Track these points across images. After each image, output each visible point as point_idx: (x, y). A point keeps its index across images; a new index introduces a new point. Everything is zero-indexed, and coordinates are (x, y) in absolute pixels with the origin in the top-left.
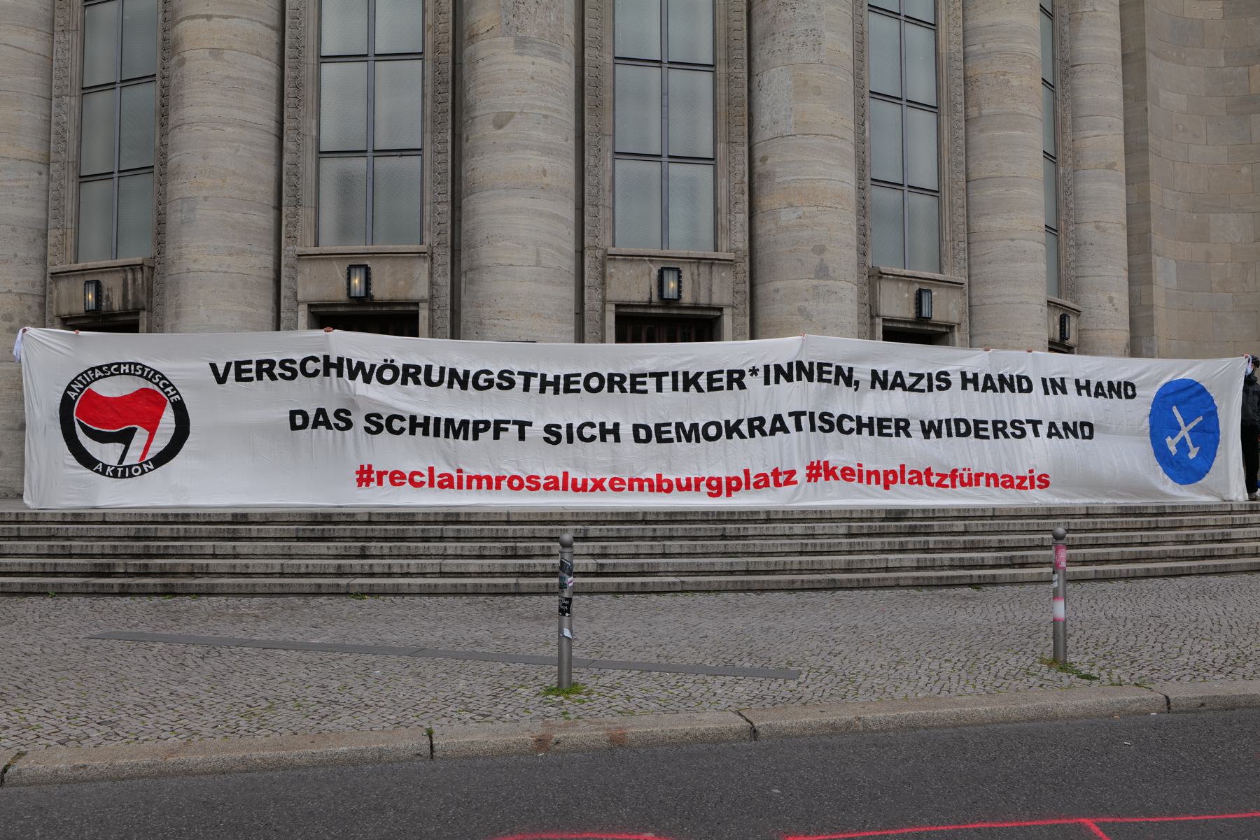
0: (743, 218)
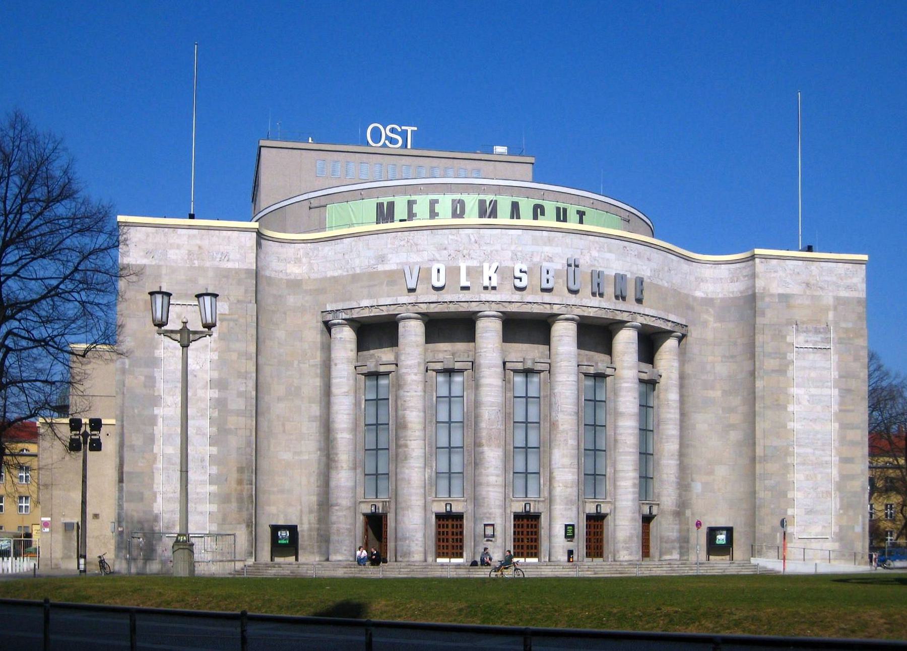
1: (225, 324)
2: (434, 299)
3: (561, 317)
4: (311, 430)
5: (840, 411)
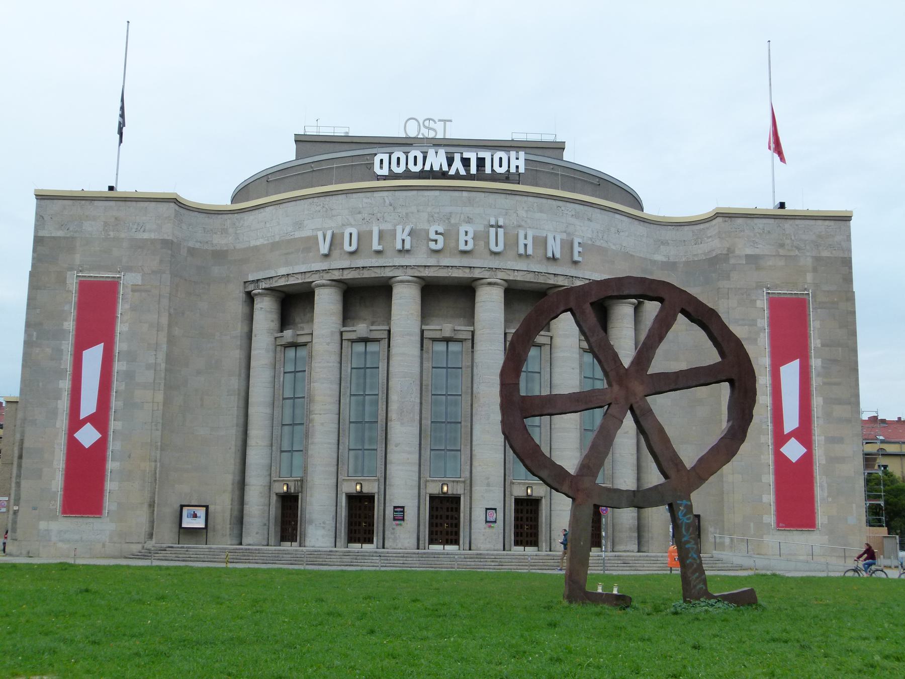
0: (468, 467)
1: (136, 294)
2: (345, 264)
3: (484, 281)
4: (233, 404)
5: (824, 384)
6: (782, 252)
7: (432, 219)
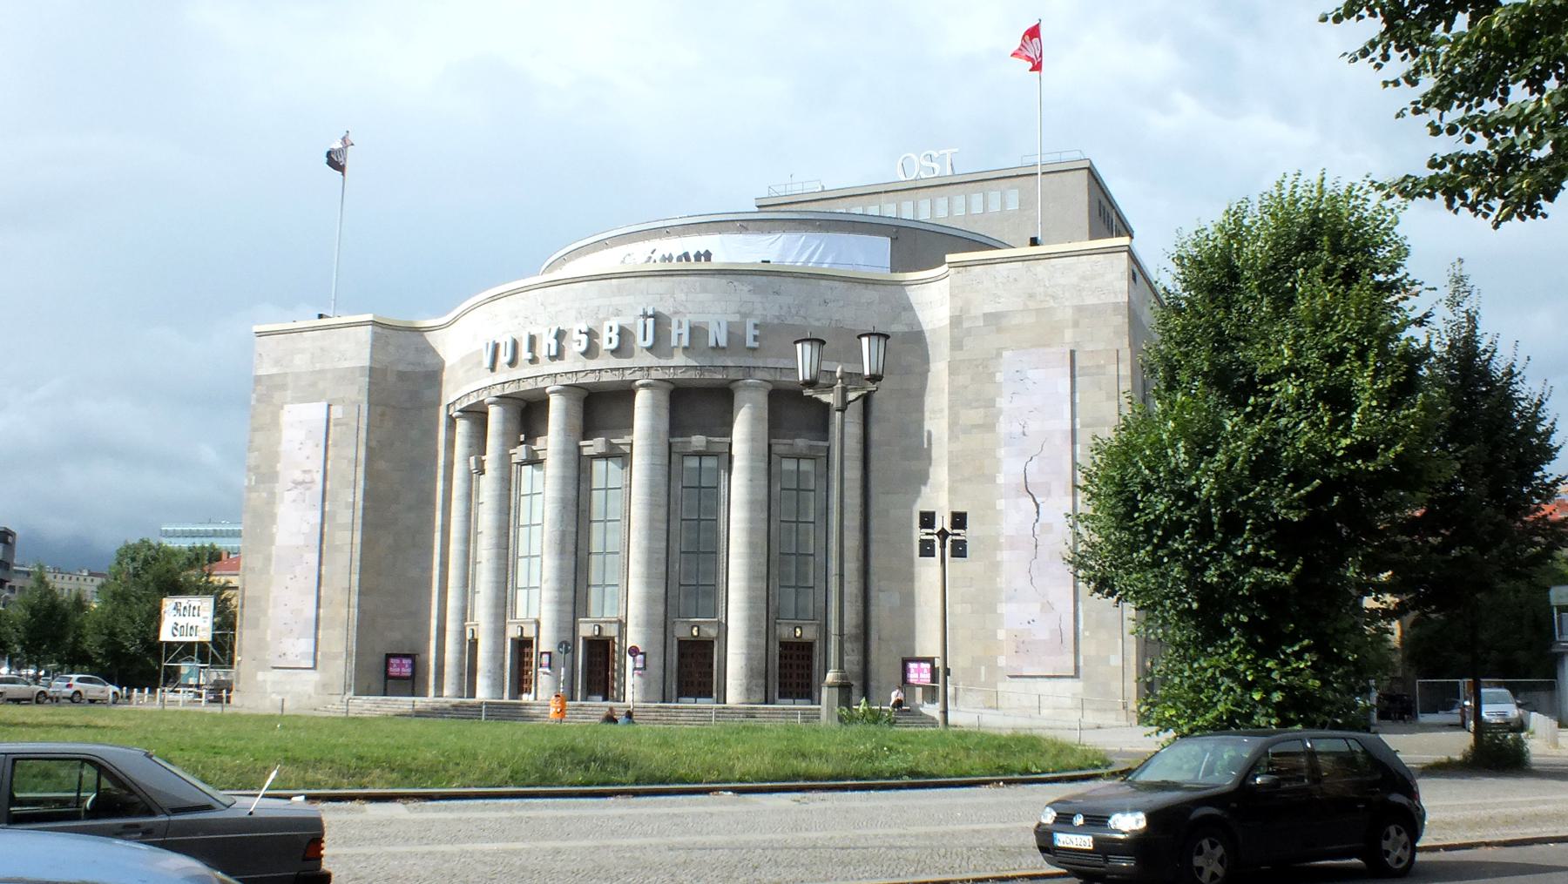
6: (1032, 305)
7: (579, 316)
